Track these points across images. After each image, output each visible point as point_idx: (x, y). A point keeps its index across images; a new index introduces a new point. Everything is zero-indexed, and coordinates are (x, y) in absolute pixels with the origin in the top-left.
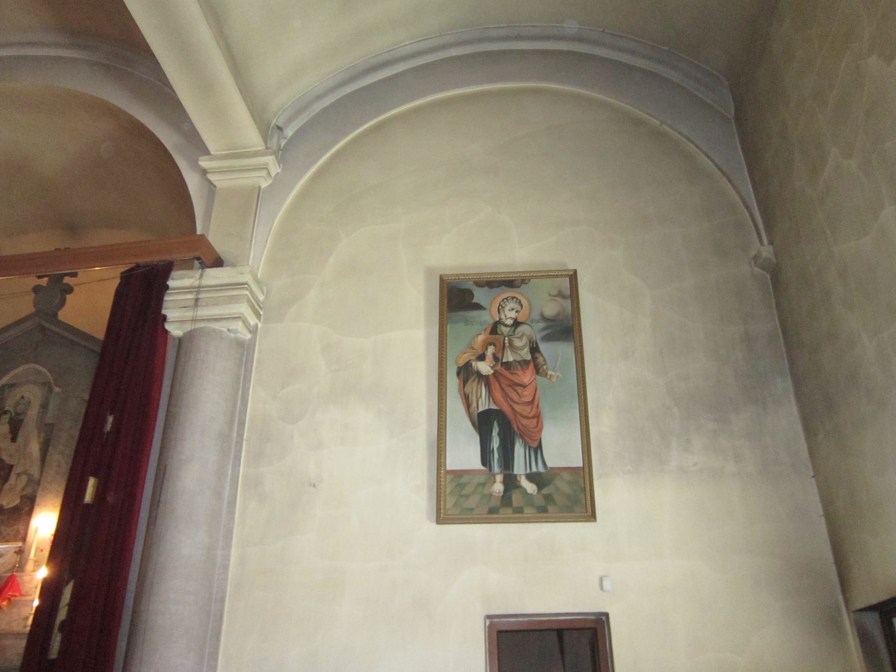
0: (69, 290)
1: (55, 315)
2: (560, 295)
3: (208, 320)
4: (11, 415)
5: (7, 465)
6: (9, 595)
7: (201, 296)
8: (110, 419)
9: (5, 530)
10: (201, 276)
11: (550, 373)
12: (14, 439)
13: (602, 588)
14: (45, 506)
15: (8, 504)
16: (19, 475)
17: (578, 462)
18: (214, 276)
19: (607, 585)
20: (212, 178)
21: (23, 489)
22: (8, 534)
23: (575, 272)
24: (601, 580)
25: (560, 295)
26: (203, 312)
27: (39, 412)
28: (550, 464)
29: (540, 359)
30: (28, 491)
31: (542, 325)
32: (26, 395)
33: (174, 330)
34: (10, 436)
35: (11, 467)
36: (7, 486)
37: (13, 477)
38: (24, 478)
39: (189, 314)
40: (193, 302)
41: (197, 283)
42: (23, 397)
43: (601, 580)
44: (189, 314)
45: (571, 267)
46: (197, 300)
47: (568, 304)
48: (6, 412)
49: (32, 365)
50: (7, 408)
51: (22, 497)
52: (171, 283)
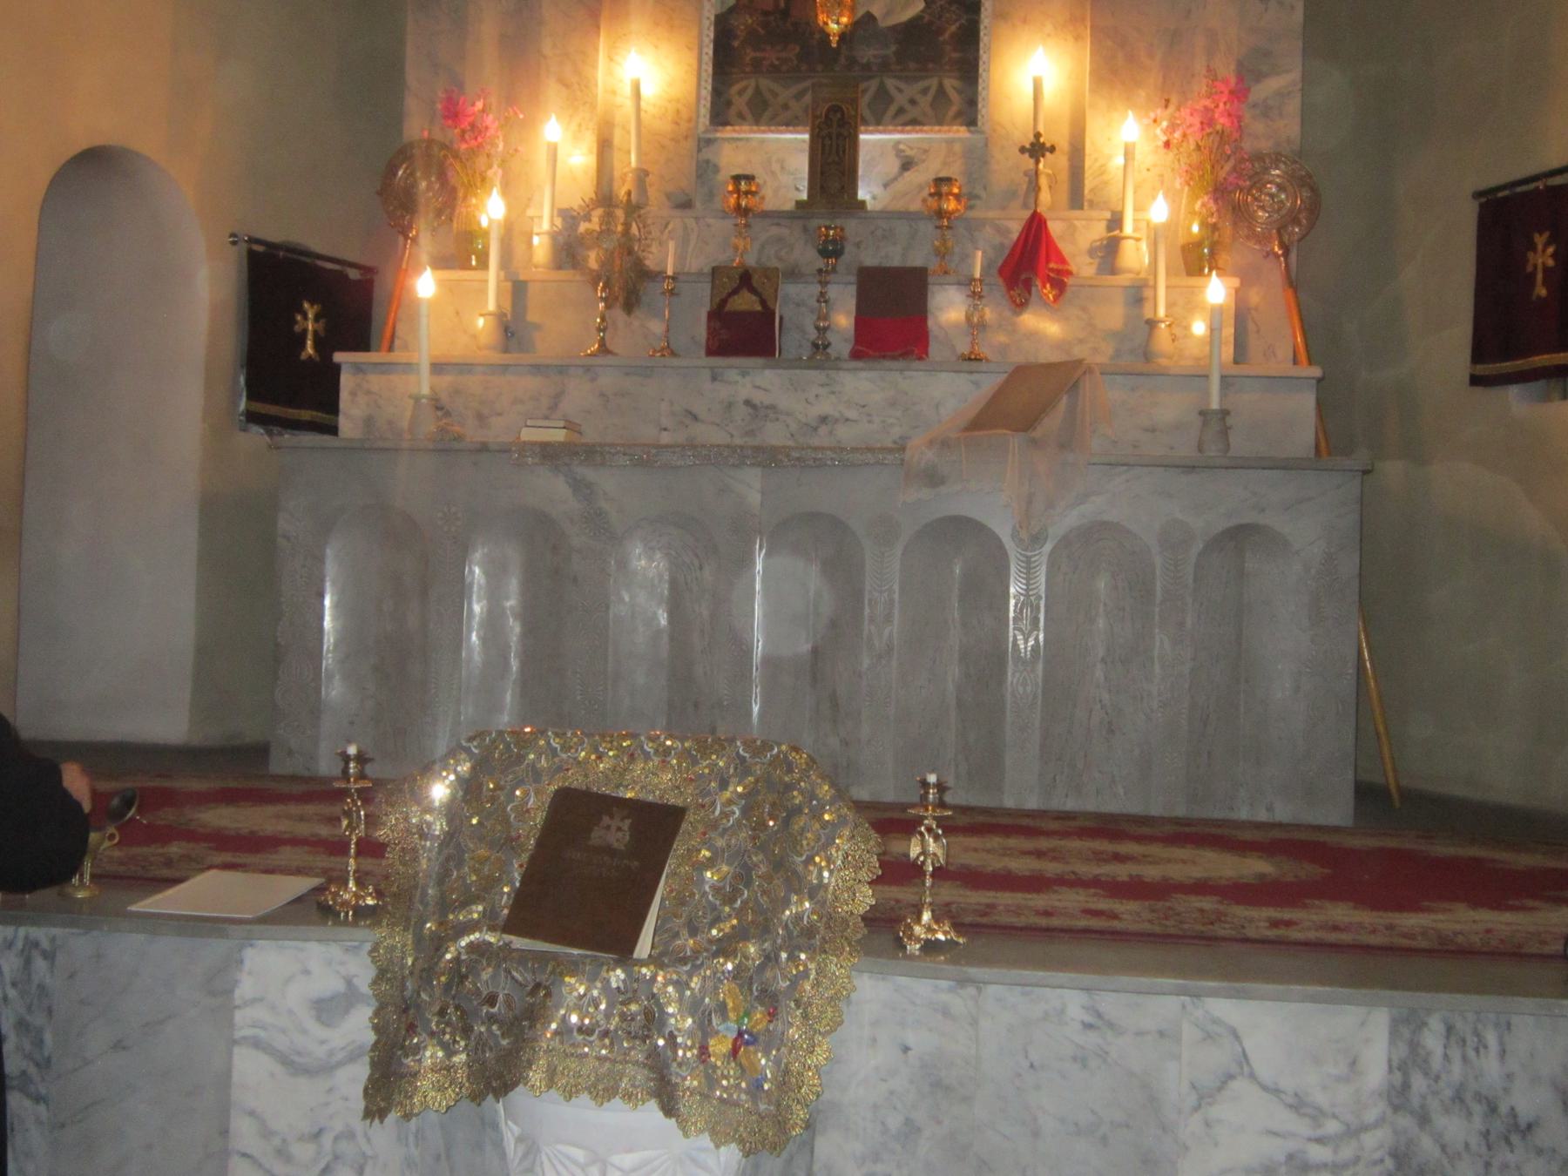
6: (1052, 270)
9: (900, 91)
14: (1025, 21)
15: (888, 13)
22: (913, 102)
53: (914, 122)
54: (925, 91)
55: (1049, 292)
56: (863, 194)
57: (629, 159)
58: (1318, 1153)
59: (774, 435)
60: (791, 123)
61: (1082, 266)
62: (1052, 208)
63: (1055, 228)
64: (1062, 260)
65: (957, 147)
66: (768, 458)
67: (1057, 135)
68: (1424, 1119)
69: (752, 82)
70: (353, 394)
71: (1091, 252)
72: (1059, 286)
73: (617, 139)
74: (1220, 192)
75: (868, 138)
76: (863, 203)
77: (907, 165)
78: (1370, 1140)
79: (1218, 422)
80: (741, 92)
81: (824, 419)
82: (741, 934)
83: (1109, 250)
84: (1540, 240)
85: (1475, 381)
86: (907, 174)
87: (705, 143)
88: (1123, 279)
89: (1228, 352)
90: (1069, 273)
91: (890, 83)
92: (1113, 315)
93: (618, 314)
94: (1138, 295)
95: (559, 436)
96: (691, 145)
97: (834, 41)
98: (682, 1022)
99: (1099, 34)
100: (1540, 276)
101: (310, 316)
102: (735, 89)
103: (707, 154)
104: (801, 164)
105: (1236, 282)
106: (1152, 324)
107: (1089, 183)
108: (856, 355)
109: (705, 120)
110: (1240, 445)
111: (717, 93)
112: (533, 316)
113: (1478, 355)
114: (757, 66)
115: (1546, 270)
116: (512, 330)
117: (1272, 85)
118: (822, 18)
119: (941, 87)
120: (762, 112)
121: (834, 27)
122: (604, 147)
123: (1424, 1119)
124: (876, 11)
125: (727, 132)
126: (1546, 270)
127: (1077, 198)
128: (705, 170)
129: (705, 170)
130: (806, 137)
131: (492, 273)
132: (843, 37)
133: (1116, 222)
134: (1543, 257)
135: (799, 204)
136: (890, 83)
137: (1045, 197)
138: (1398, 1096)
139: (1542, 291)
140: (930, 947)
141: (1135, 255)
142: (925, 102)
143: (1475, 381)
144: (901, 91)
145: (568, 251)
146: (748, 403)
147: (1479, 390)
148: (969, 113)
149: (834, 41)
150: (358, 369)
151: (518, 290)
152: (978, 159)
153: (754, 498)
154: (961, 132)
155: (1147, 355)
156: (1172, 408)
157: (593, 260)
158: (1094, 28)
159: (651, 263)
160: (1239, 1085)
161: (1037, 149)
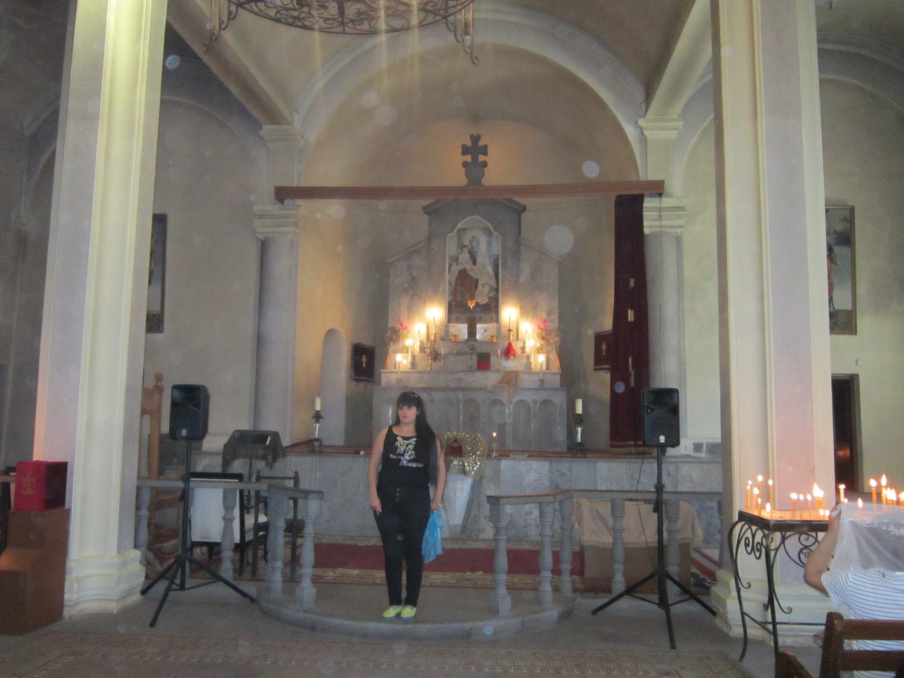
0: (485, 164)
1: (480, 183)
2: (845, 219)
3: (664, 227)
4: (469, 248)
5: (475, 279)
7: (663, 213)
8: (632, 281)
10: (660, 201)
11: (838, 262)
12: (475, 263)
13: (857, 364)
16: (483, 285)
17: (849, 307)
18: (666, 202)
19: (860, 362)
20: (645, 132)
21: (488, 294)
23: (853, 207)
24: (857, 361)
25: (845, 219)
26: (664, 223)
27: (487, 248)
28: (836, 308)
29: (833, 255)
30: (492, 294)
31: (834, 236)
32: (475, 236)
33: (646, 231)
34: (471, 261)
35: (477, 280)
36: (477, 291)
37: (480, 287)
38: (487, 289)
39: (657, 223)
40: (657, 217)
41: (658, 205)
42: (474, 237)
43: (857, 361)
44: (657, 223)
45: (850, 203)
46: (660, 216)
47: (848, 225)
48: (465, 246)
49: (475, 217)
50: (465, 244)
51: (488, 298)
52: (645, 205)
53: (486, 323)
54: (489, 316)
55: (512, 357)
56: (477, 338)
57: (433, 331)
58: (541, 478)
59: (463, 385)
60: (463, 323)
61: (519, 352)
62: (513, 340)
63: (513, 344)
64: (515, 351)
65: (495, 327)
66: (463, 389)
67: (513, 327)
68: (553, 474)
69: (455, 315)
70: (384, 377)
71: (520, 348)
72: (514, 356)
73: (430, 326)
74: (543, 338)
75: (478, 326)
76: (478, 340)
77: (485, 331)
78: (547, 476)
79: (542, 381)
80: (453, 316)
81: (472, 381)
82: (473, 455)
83: (523, 349)
84: (604, 344)
85: (595, 369)
86: (486, 333)
87: (446, 326)
88: (526, 355)
89: (544, 367)
90: (516, 354)
91: (482, 315)
92: (524, 361)
93: (433, 362)
94: (528, 357)
95: (425, 386)
96: (444, 327)
97: (471, 308)
98: (466, 464)
99: (521, 307)
100: (604, 351)
101: (364, 357)
102: (453, 316)
103: (447, 328)
104: (466, 331)
105: (546, 355)
106: (531, 363)
107: (520, 337)
108: (478, 369)
109: (447, 322)
110: (547, 385)
111: (449, 317)
112: (416, 362)
113: (595, 365)
114: (456, 311)
115: (605, 350)
116: (413, 364)
117: (553, 317)
118: (469, 304)
119: (492, 316)
120: (458, 321)
121: (471, 306)
122: (428, 328)
123: (553, 474)
124: (479, 301)
125: (451, 325)
126: (605, 350)
127: (517, 339)
128: (447, 332)
129: (447, 332)
130: (466, 325)
131: (409, 354)
132: (473, 307)
133: (524, 343)
134: (604, 347)
135: (466, 340)
136: (482, 315)
137: (512, 338)
138: (550, 471)
139: (604, 354)
140: (495, 456)
141: (527, 350)
142: (488, 319)
143: (595, 369)
144: (484, 316)
145: (422, 349)
146: (458, 378)
147: (595, 371)
148: (497, 320)
149: (471, 308)
150: (384, 372)
151: (414, 357)
152: (499, 329)
153: (461, 397)
154: (496, 325)
155: (530, 369)
156: (536, 378)
157: (428, 351)
158: (520, 306)
159: (439, 352)
160: (532, 471)
161: (510, 330)
